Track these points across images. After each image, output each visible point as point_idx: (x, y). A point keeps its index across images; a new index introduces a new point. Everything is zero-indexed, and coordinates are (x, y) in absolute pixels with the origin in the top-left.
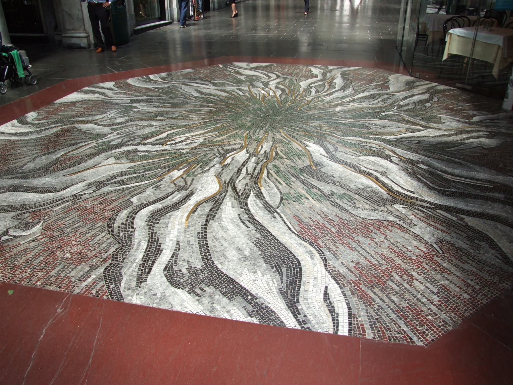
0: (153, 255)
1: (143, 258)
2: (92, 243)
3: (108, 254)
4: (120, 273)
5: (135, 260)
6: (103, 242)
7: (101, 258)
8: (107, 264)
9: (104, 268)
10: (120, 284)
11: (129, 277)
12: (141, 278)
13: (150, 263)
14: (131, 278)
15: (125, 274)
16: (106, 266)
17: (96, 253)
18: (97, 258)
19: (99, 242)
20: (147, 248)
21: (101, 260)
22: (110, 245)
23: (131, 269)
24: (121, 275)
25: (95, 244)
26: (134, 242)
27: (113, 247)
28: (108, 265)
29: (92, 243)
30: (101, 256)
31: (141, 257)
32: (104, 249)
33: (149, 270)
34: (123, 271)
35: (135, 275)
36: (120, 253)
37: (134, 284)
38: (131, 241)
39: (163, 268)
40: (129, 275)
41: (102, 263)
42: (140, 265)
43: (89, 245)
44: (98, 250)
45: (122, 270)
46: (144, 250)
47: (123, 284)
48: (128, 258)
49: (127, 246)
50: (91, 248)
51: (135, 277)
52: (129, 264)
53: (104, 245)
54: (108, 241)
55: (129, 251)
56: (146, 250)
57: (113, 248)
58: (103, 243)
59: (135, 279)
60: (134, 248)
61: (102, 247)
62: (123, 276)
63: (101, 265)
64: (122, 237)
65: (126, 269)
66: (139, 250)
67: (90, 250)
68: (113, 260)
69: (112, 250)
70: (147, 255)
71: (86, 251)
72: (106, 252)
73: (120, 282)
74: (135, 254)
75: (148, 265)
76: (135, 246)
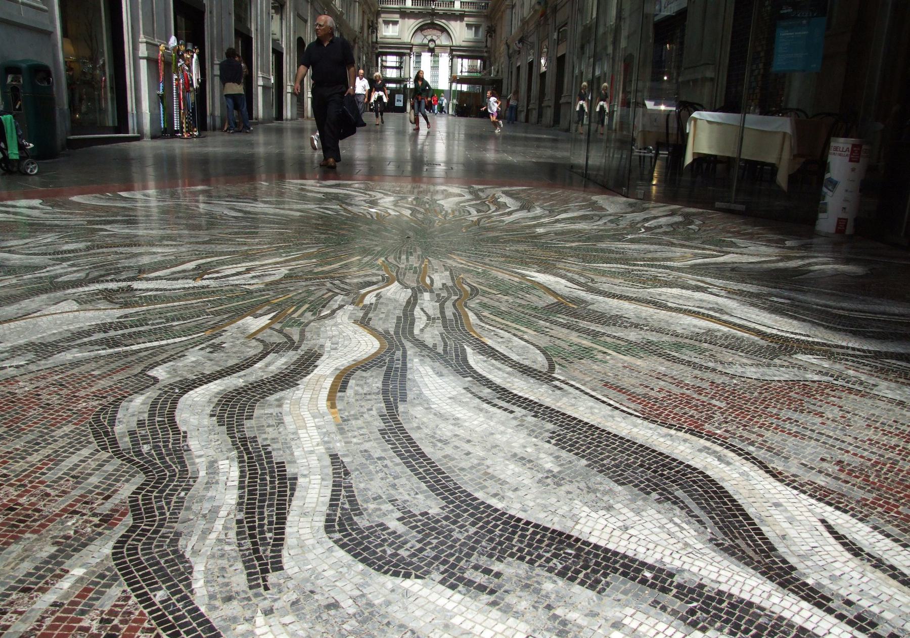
0: (272, 494)
1: (240, 504)
2: (50, 476)
3: (117, 502)
4: (175, 552)
5: (215, 511)
6: (89, 471)
7: (95, 515)
8: (120, 530)
9: (111, 544)
10: (189, 586)
11: (212, 561)
12: (259, 558)
13: (270, 516)
14: (224, 563)
15: (195, 552)
16: (117, 537)
17: (70, 502)
18: (78, 516)
19: (74, 473)
20: (242, 476)
21: (96, 520)
22: (115, 478)
23: (213, 536)
24: (183, 556)
25: (60, 478)
26: (194, 464)
27: (127, 481)
28: (123, 532)
29: (50, 476)
30: (92, 509)
31: (234, 502)
32: (97, 491)
33: (276, 534)
34: (187, 545)
35: (234, 554)
36: (156, 497)
37: (239, 579)
38: (182, 463)
39: (322, 524)
40: (213, 556)
41: (100, 530)
42: (239, 522)
43: (42, 482)
44: (77, 493)
45: (181, 542)
46: (236, 483)
47: (198, 584)
48: (188, 509)
49: (175, 475)
50: (48, 490)
51: (235, 558)
52: (201, 524)
53: (94, 480)
54: (104, 468)
55: (188, 490)
56: (241, 482)
57: (127, 485)
58: (90, 475)
59: (240, 565)
60: (199, 480)
61: (90, 484)
62: (191, 559)
63: (100, 534)
64: (152, 456)
65: (194, 538)
66: (217, 483)
67: (48, 495)
68: (137, 517)
69: (126, 491)
70: (251, 493)
71: (34, 499)
72: (107, 498)
73: (187, 579)
74: (209, 494)
75: (266, 521)
76: (202, 473)
